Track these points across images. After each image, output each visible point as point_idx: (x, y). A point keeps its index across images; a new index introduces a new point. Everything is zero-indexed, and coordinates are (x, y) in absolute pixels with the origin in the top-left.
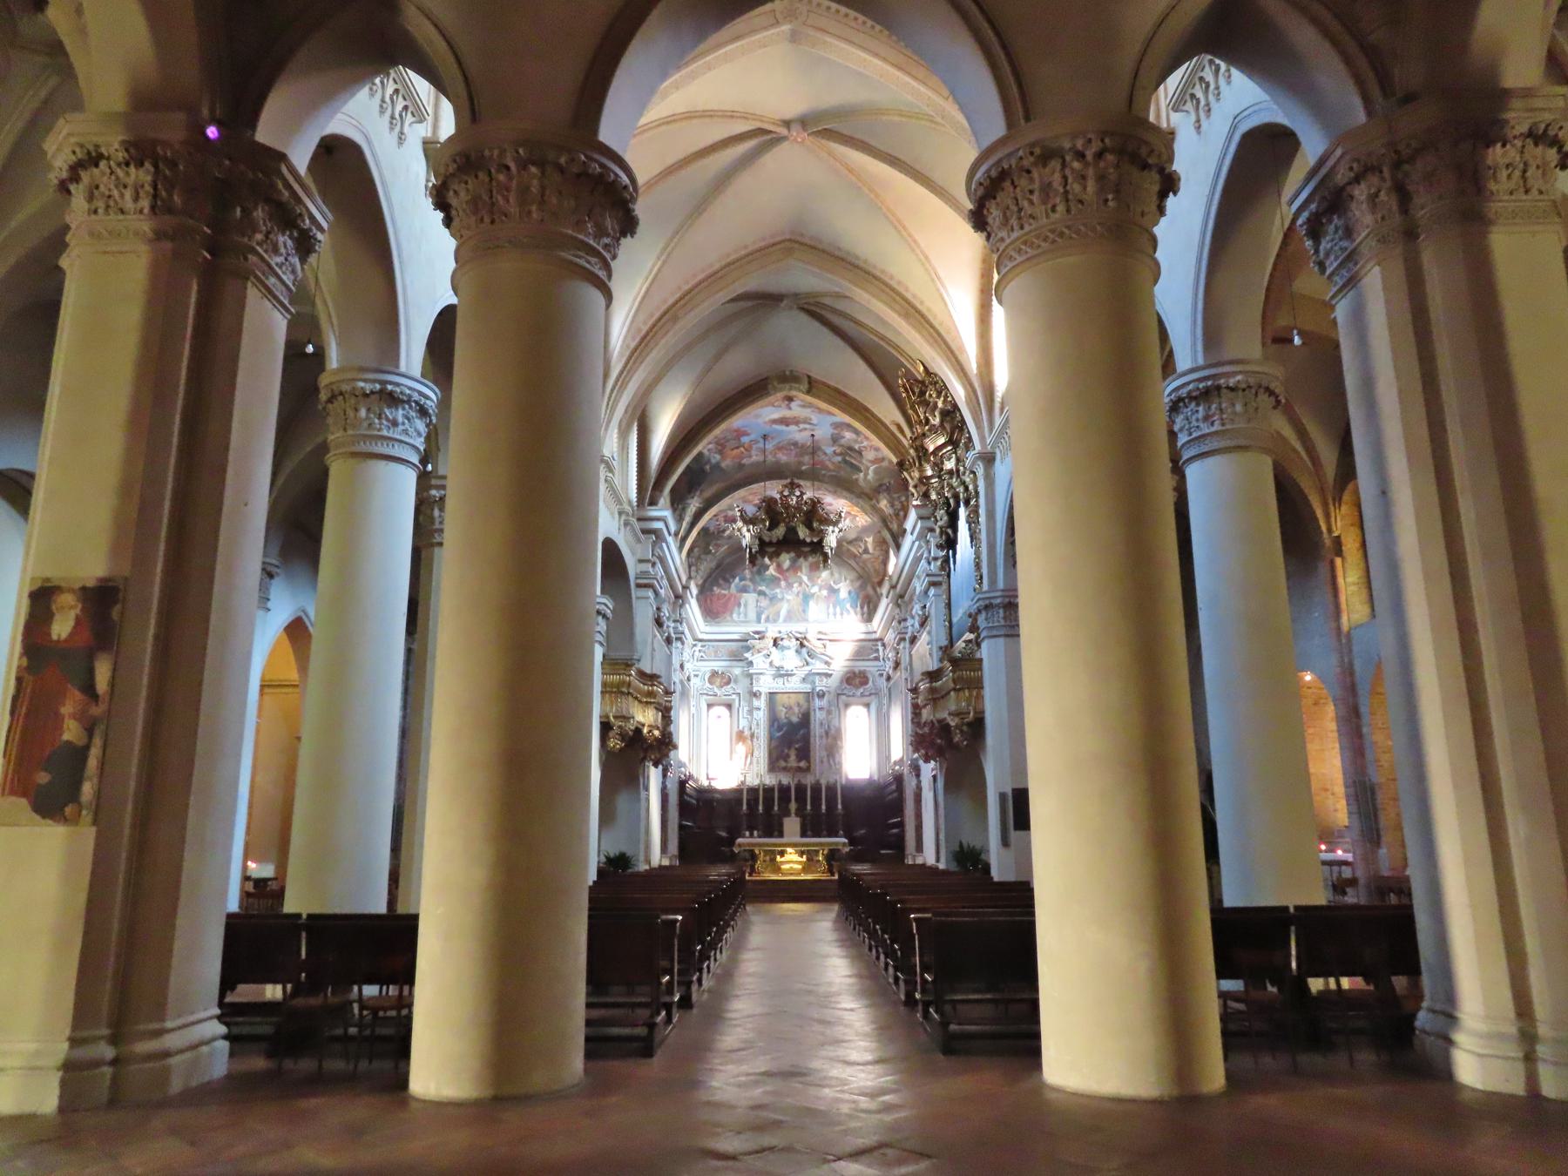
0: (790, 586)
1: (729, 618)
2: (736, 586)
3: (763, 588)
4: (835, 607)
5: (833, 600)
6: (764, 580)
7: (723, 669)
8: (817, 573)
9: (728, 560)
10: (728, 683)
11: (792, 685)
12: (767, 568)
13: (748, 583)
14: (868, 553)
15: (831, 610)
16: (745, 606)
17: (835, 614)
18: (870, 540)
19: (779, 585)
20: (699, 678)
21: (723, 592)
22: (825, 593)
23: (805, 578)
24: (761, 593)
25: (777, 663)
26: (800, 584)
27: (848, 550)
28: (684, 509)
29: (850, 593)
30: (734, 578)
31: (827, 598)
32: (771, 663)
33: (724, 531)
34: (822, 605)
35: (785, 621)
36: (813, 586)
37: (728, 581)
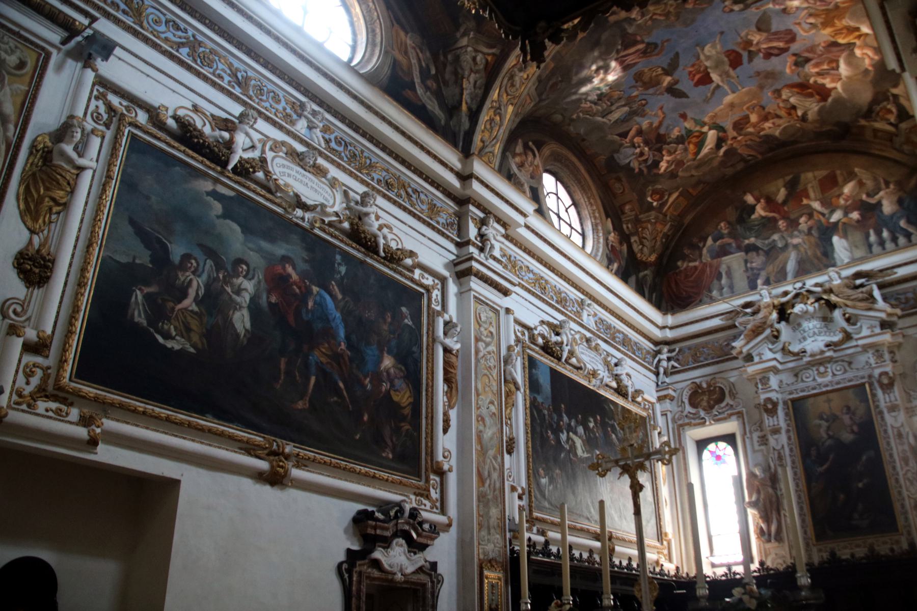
0: (793, 224)
1: (705, 299)
2: (709, 251)
3: (752, 240)
4: (879, 233)
5: (872, 221)
6: (750, 229)
7: (709, 378)
8: (835, 191)
9: (688, 219)
10: (721, 399)
11: (829, 378)
12: (752, 209)
13: (727, 240)
15: (873, 238)
16: (729, 274)
17: (882, 243)
19: (776, 229)
20: (675, 402)
21: (692, 264)
22: (855, 215)
23: (816, 205)
25: (795, 348)
26: (810, 216)
27: (876, 131)
28: (457, 59)
29: (900, 202)
31: (861, 224)
32: (785, 350)
33: (656, 164)
34: (858, 236)
35: (795, 277)
36: (832, 212)
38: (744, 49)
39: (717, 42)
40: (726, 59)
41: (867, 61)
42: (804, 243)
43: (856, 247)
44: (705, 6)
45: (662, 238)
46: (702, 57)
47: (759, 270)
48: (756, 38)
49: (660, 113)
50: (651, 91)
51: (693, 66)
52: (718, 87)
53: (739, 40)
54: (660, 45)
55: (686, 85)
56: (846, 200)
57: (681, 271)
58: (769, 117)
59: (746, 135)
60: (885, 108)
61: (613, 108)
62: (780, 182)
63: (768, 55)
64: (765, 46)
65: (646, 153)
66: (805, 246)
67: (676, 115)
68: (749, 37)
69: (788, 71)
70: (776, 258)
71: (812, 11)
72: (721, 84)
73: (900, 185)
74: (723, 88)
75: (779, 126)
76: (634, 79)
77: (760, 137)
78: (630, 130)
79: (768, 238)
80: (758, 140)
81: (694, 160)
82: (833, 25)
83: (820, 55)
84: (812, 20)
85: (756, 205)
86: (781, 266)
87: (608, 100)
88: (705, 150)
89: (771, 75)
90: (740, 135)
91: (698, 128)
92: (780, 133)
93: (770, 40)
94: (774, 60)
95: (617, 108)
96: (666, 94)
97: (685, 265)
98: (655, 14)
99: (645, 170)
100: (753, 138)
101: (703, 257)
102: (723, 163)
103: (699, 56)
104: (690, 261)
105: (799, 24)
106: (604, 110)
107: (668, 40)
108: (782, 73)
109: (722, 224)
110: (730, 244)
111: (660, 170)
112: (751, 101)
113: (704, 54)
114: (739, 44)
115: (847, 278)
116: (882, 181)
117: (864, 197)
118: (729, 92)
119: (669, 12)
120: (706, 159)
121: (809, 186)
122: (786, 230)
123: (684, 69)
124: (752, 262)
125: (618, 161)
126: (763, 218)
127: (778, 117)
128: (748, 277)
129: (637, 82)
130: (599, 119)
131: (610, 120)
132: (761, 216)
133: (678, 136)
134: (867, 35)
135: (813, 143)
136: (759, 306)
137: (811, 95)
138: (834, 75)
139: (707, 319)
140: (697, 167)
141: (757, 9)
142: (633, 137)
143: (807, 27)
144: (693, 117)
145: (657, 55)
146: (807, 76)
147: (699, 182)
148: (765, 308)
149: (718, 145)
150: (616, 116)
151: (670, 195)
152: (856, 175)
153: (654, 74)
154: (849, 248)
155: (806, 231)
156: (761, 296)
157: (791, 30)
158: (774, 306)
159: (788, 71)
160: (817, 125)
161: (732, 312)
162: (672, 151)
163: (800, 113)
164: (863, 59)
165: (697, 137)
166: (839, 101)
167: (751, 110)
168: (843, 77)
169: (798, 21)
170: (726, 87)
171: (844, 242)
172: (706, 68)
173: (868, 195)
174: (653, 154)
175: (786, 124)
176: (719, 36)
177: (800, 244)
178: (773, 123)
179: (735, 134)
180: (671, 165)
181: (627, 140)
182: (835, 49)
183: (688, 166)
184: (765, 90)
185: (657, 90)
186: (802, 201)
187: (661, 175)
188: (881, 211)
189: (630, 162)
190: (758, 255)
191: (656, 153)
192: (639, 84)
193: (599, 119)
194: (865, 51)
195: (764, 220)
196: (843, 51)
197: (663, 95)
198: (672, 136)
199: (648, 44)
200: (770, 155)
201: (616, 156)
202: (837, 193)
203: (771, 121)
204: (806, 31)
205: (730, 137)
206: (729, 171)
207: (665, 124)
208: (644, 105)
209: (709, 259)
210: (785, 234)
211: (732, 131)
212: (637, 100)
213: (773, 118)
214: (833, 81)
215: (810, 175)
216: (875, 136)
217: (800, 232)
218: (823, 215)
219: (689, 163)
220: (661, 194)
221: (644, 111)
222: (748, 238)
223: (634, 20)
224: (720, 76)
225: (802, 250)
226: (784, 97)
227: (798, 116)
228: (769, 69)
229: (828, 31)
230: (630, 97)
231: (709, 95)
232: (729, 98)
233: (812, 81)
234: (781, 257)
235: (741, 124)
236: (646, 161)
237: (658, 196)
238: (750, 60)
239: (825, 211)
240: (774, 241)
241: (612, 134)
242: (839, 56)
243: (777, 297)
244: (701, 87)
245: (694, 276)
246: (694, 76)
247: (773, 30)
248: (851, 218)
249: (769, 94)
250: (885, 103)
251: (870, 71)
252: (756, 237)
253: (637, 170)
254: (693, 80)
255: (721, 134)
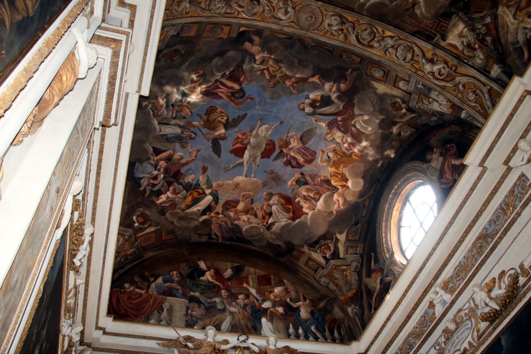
0: (233, 297)
2: (156, 287)
3: (197, 294)
4: (296, 329)
6: (197, 286)
9: (149, 254)
12: (203, 273)
14: (339, 258)
15: (291, 330)
16: (170, 310)
18: (342, 237)
21: (137, 290)
22: (280, 310)
23: (253, 291)
24: (192, 299)
27: (310, 259)
29: (312, 313)
30: (156, 278)
31: (284, 317)
33: (159, 193)
34: (281, 325)
36: (264, 300)
37: (147, 281)
38: (280, 147)
39: (273, 127)
40: (264, 146)
41: (336, 206)
42: (239, 313)
43: (279, 332)
44: (295, 92)
45: (122, 257)
46: (254, 132)
47: (196, 318)
48: (294, 144)
49: (194, 155)
50: (205, 131)
51: (244, 134)
52: (242, 164)
53: (284, 138)
54: (245, 98)
55: (226, 146)
56: (276, 297)
57: (125, 292)
58: (250, 213)
59: (225, 216)
60: (327, 244)
61: (173, 122)
62: (229, 265)
63: (288, 163)
64: (292, 154)
65: (159, 179)
66: (239, 316)
67: (201, 165)
68: (291, 140)
69: (289, 183)
70: (216, 315)
71: (338, 148)
72: (245, 163)
73: (314, 303)
74: (244, 167)
75: (250, 223)
76: (207, 110)
77: (232, 224)
78: (165, 151)
79: (212, 299)
80: (230, 225)
81: (183, 210)
82: (337, 168)
83: (315, 185)
84: (331, 155)
85: (207, 271)
86: (216, 323)
87: (176, 112)
88: (195, 209)
89: (277, 179)
90: (223, 214)
91: (204, 187)
92: (246, 230)
93: (299, 152)
94: (289, 168)
95: (174, 125)
96: (210, 141)
97: (131, 289)
98: (268, 69)
99: (148, 192)
100: (227, 222)
101: (150, 290)
102: (196, 228)
103: (254, 129)
104: (137, 288)
105: (323, 152)
106: (166, 118)
107: (252, 99)
108: (285, 182)
109: (175, 273)
110: (177, 289)
111: (158, 200)
112: (250, 192)
113: (258, 130)
114: (281, 140)
115: (279, 349)
116: (301, 295)
117: (288, 300)
118: (244, 173)
119: (275, 76)
120: (190, 217)
121: (250, 276)
122: (226, 298)
123: (237, 132)
124: (193, 311)
125: (135, 170)
126: (210, 282)
127: (256, 216)
128: (187, 321)
129: (205, 114)
130: (156, 122)
131: (161, 131)
132: (208, 280)
133: (189, 182)
134: (348, 187)
135: (261, 250)
136: (202, 344)
137: (287, 211)
138: (313, 204)
139: (145, 337)
140: (181, 218)
141: (316, 121)
142: (162, 159)
143: (325, 157)
144: (209, 176)
145: (236, 104)
146: (297, 195)
147: (172, 232)
148: (209, 346)
149: (204, 212)
150: (168, 130)
151: (150, 226)
152: (284, 284)
153: (219, 119)
154: (273, 331)
155: (242, 306)
156: (206, 335)
157: (316, 153)
158: (214, 349)
159: (289, 183)
160: (274, 237)
161: (171, 340)
162: (177, 192)
163: (270, 222)
164: (336, 204)
165: (199, 194)
166: (303, 225)
167: (244, 199)
168: (316, 209)
169: (324, 149)
170: (245, 169)
171: (269, 323)
172: (249, 142)
173: (291, 300)
174: (163, 184)
175: (255, 225)
176: (278, 123)
177: (235, 313)
178: (249, 219)
179: (220, 210)
180: (168, 202)
181: (156, 158)
182: (326, 186)
183: (176, 212)
184: (265, 189)
185: (208, 134)
186: (243, 284)
187: (156, 205)
188: (299, 315)
189: (142, 178)
190: (199, 307)
191: (165, 184)
192: (205, 117)
193: (156, 122)
194: (339, 199)
195: (210, 284)
196: (329, 190)
197: (209, 141)
198: (186, 180)
199: (242, 90)
200: (228, 243)
201: (137, 164)
202: (270, 290)
203: (248, 216)
204: (322, 162)
205: (216, 211)
206: (195, 238)
207: (188, 167)
208: (191, 139)
209: (155, 293)
210: (225, 301)
211: (221, 206)
212: (192, 129)
213: (251, 215)
214: (309, 208)
215: (252, 270)
216: (306, 264)
217: (237, 303)
218: (258, 300)
219: (178, 211)
220: (145, 220)
221: (187, 143)
222: (194, 292)
223: (255, 60)
224: (250, 156)
225: (237, 317)
226: (271, 202)
227: (267, 223)
228: (280, 174)
229: (332, 170)
230: (190, 123)
231: (232, 166)
232: (240, 179)
233: (296, 200)
234: (218, 316)
235: (230, 206)
236: (154, 185)
237: (142, 220)
238: (276, 159)
239: (259, 298)
240: (215, 302)
241: (150, 144)
242: (324, 193)
243: (219, 343)
244: (233, 155)
245: (137, 301)
246: (237, 143)
247: (307, 146)
248: (278, 311)
249: (265, 193)
250: (329, 241)
251: (333, 214)
252: (201, 293)
253: (142, 188)
254: (234, 145)
255: (213, 203)
